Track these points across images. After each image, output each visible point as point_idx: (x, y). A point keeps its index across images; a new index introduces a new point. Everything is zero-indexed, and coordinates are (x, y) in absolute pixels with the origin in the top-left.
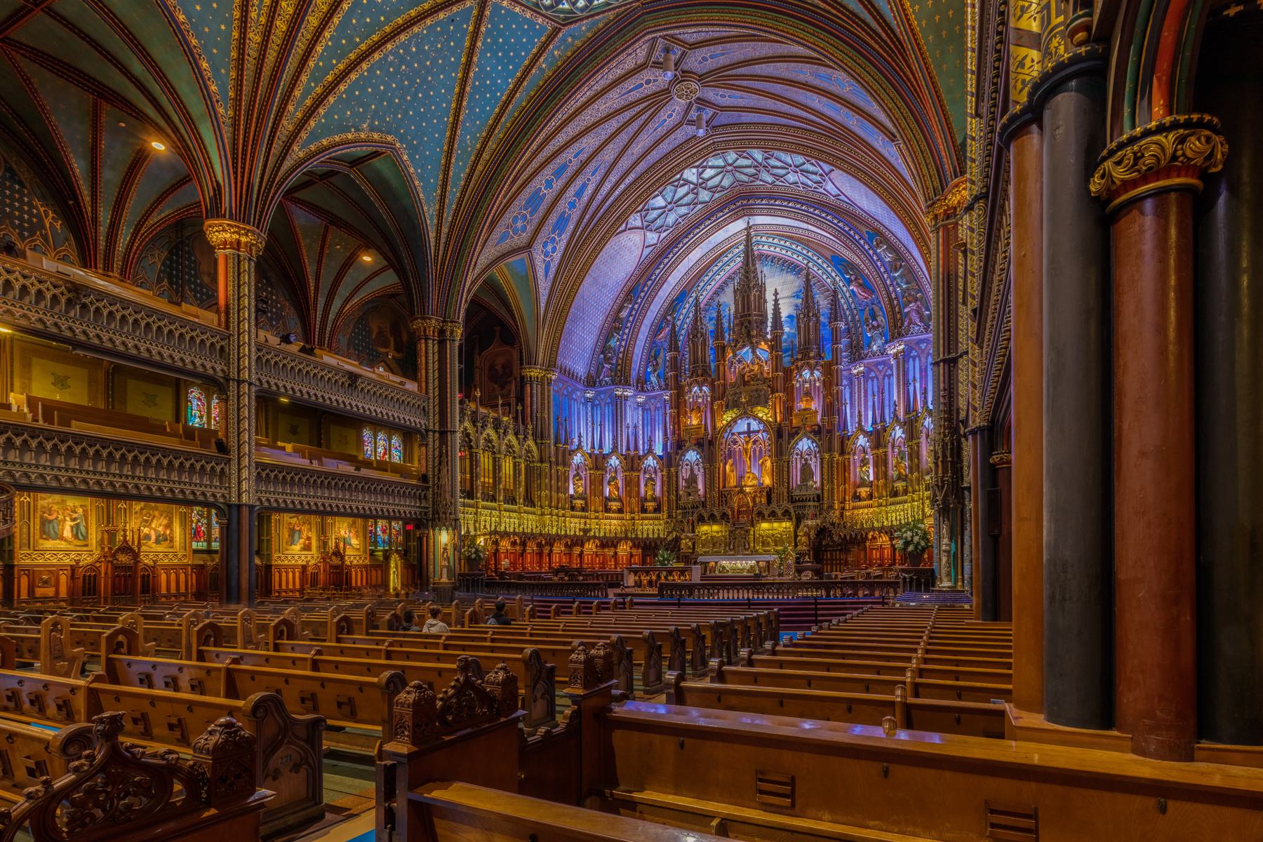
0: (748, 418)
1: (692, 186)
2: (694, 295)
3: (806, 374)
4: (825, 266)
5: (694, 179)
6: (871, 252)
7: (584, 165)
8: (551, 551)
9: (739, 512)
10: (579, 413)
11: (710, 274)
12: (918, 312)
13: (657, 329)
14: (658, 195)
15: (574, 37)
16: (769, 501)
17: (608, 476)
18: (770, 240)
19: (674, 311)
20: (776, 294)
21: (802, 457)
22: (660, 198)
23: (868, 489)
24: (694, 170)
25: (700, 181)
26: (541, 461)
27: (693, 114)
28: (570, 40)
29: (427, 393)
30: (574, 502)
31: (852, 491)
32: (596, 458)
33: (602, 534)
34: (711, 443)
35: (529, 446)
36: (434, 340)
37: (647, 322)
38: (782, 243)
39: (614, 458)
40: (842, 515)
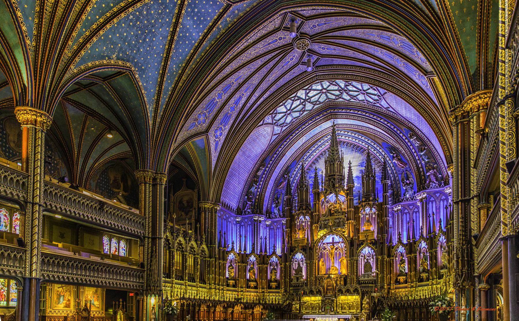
0: (333, 234)
1: (302, 101)
2: (301, 163)
3: (368, 210)
4: (378, 148)
5: (303, 97)
6: (407, 141)
7: (240, 86)
8: (215, 310)
9: (327, 289)
10: (232, 230)
11: (310, 152)
12: (435, 175)
13: (278, 183)
14: (282, 105)
15: (239, 10)
16: (345, 283)
17: (249, 267)
18: (346, 133)
19: (289, 172)
20: (350, 163)
21: (365, 258)
22: (283, 106)
23: (404, 277)
24: (304, 91)
25: (307, 98)
26: (210, 257)
27: (305, 59)
28: (236, 12)
29: (145, 214)
30: (229, 281)
31: (395, 278)
32: (242, 256)
33: (245, 301)
34: (311, 249)
35: (203, 248)
36: (150, 184)
37: (273, 178)
38: (353, 135)
39: (253, 256)
40: (389, 292)
